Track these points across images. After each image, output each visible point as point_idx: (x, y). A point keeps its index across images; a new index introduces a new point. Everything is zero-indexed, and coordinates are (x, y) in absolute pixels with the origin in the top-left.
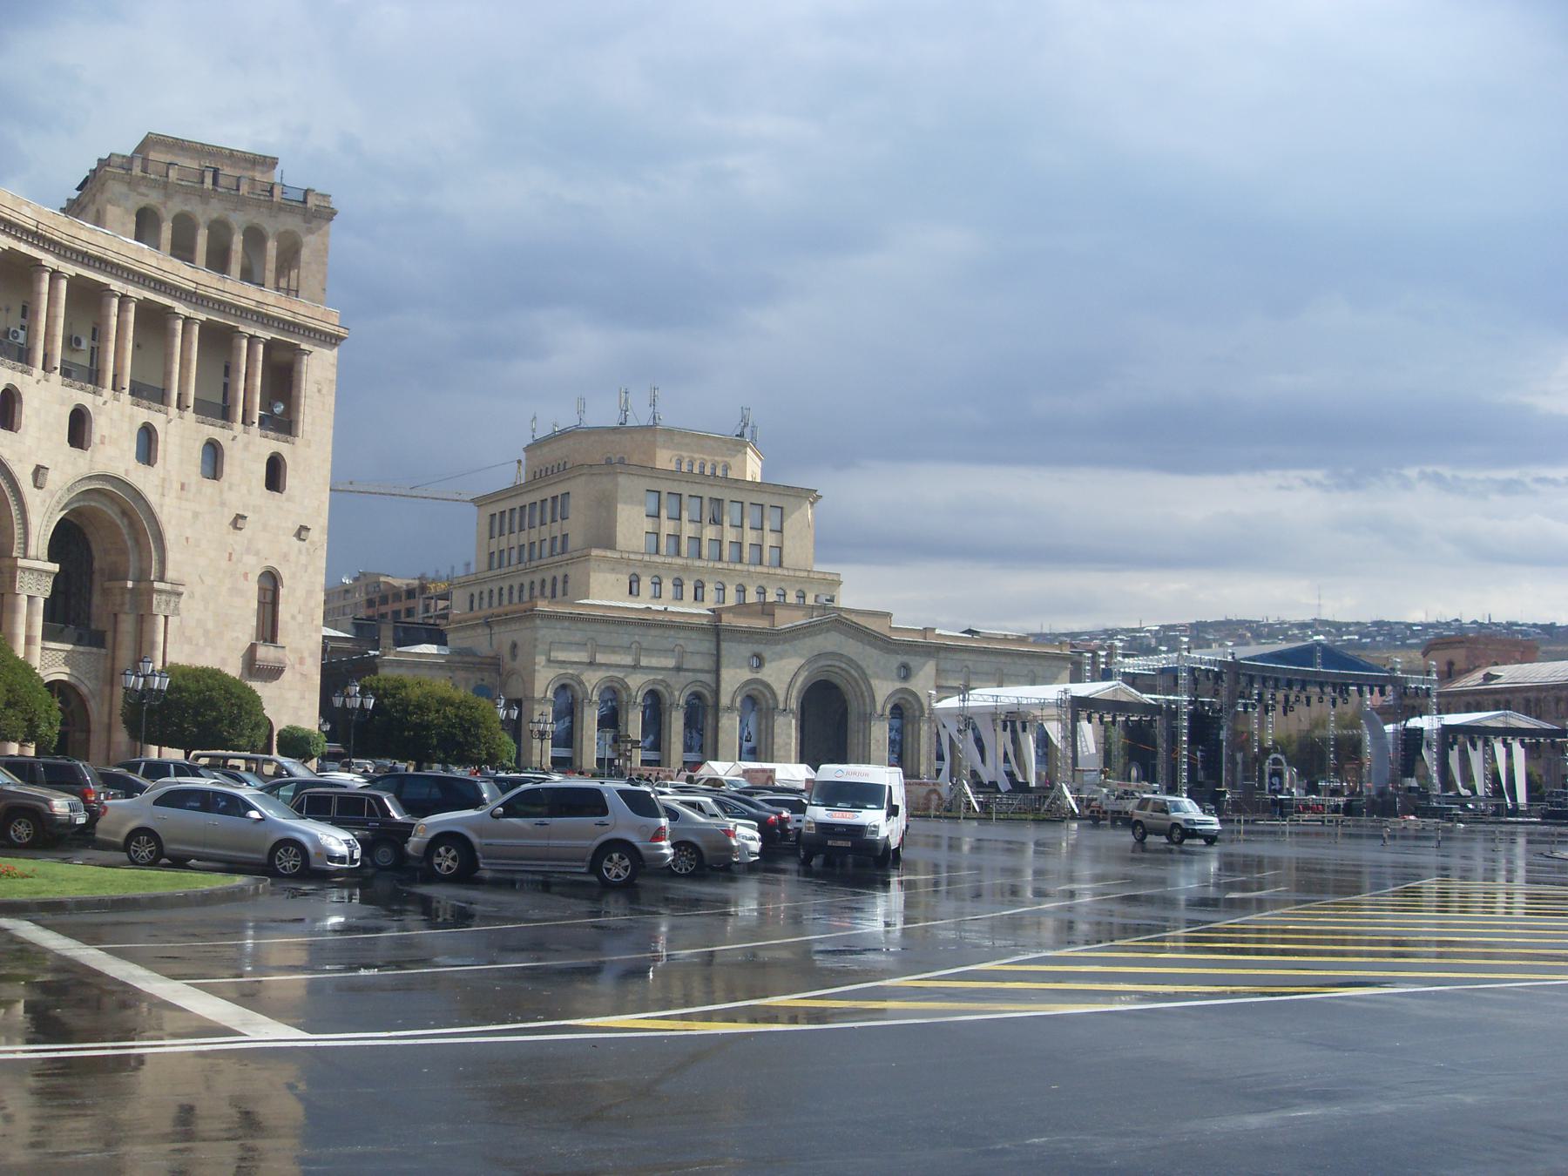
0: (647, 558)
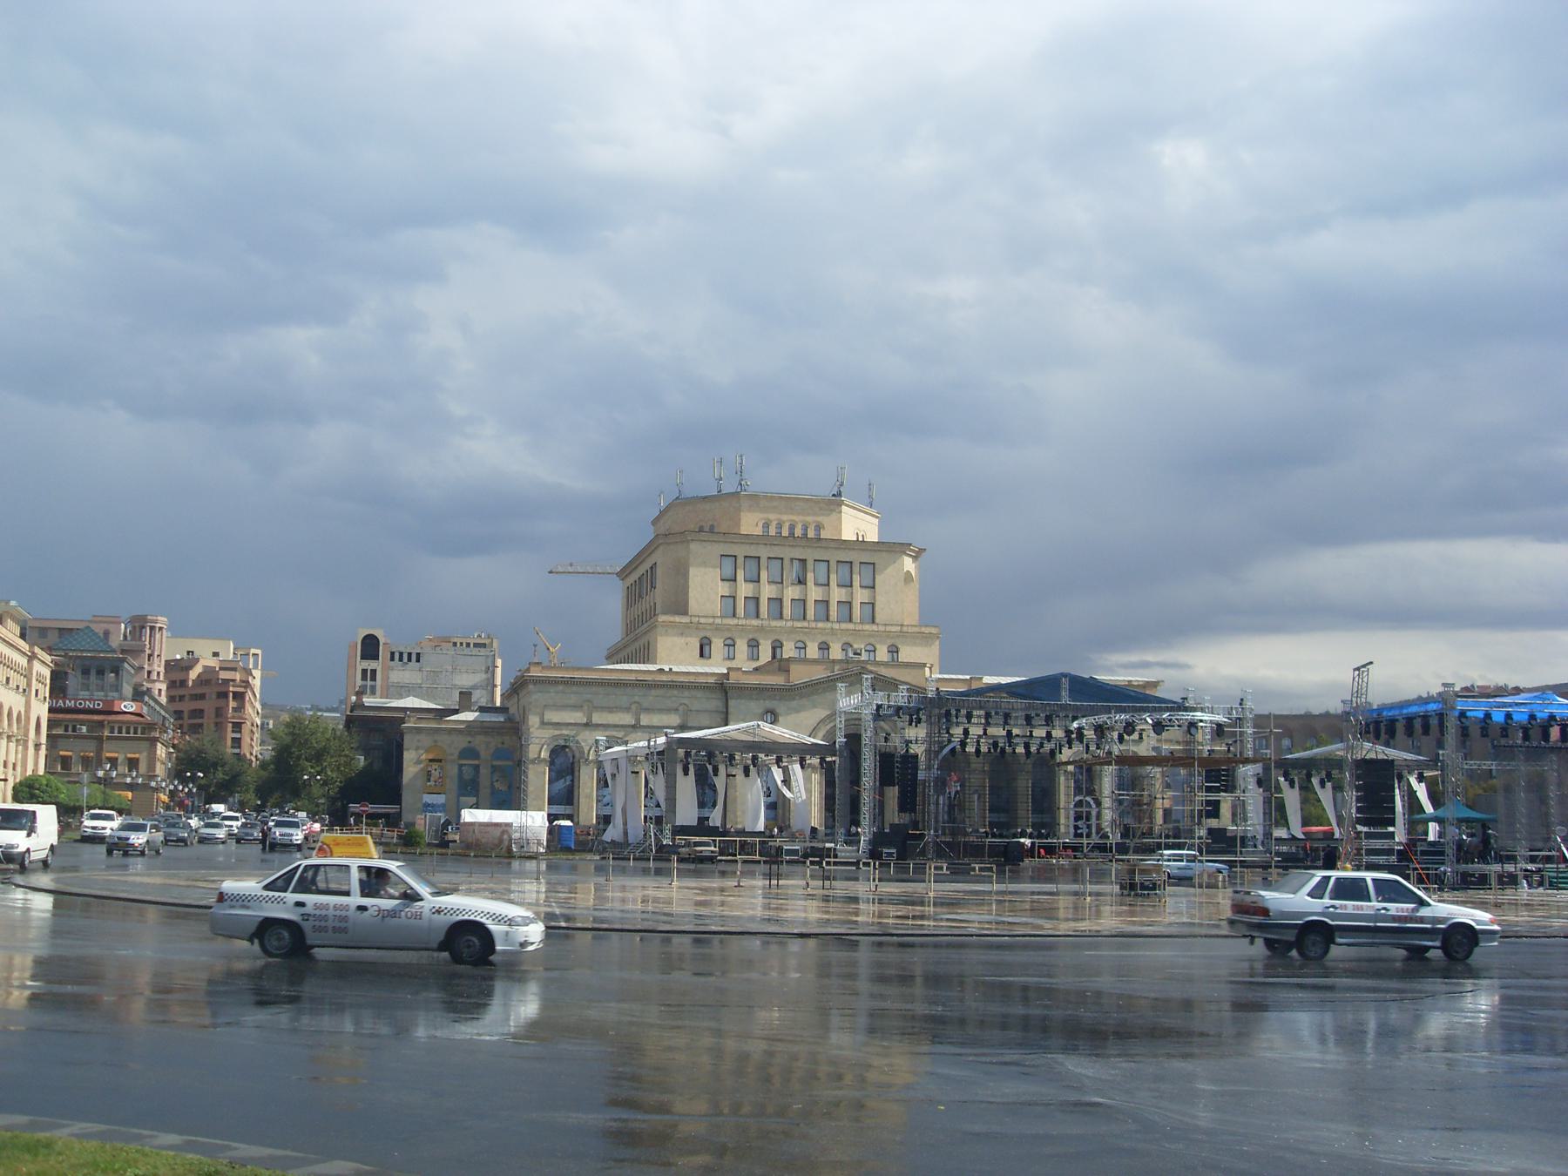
0: (718, 621)
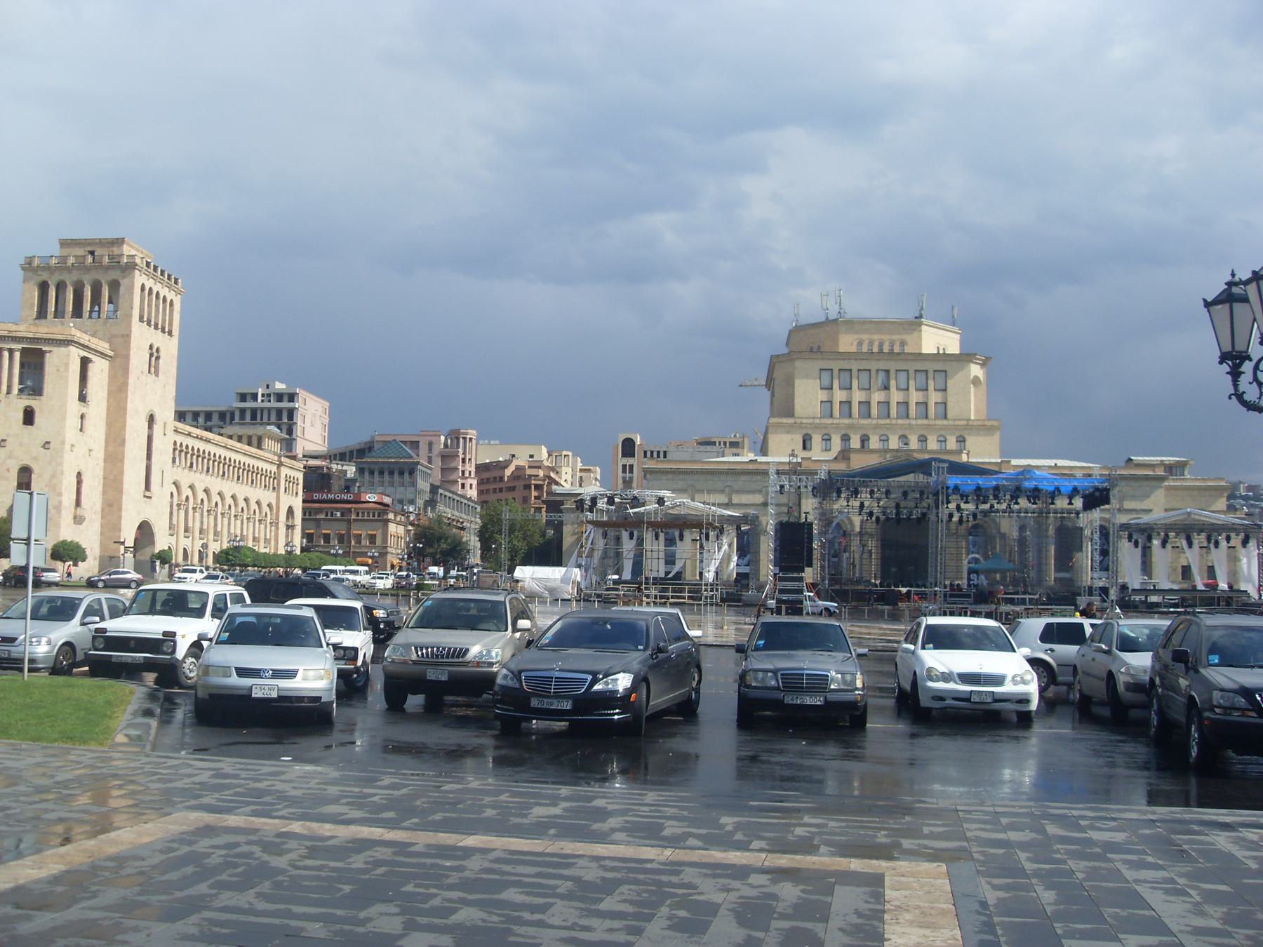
0: (817, 421)
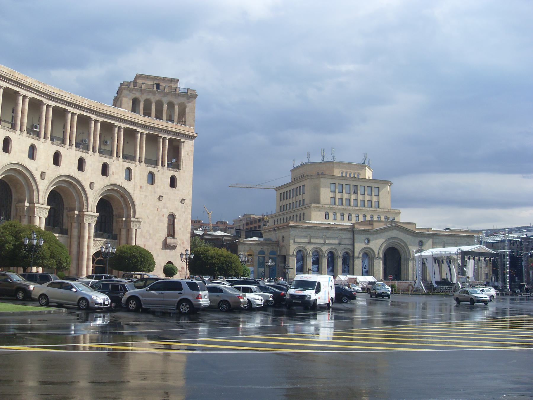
0: (331, 206)
